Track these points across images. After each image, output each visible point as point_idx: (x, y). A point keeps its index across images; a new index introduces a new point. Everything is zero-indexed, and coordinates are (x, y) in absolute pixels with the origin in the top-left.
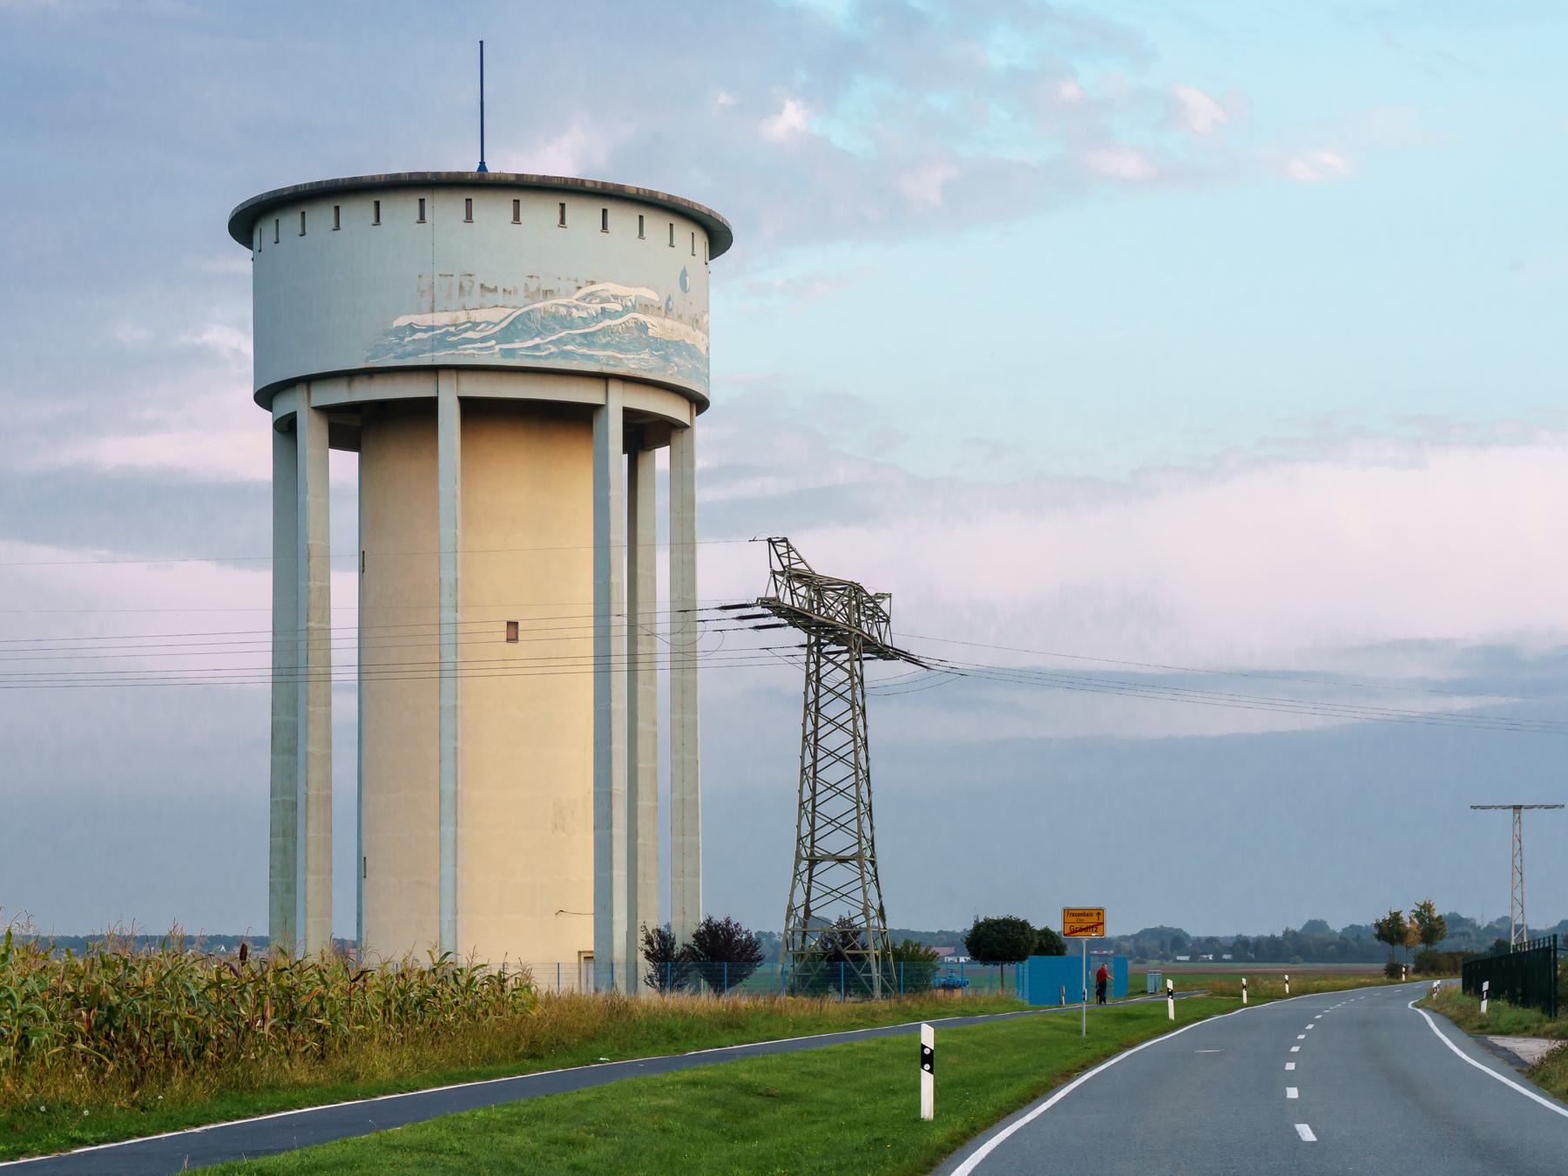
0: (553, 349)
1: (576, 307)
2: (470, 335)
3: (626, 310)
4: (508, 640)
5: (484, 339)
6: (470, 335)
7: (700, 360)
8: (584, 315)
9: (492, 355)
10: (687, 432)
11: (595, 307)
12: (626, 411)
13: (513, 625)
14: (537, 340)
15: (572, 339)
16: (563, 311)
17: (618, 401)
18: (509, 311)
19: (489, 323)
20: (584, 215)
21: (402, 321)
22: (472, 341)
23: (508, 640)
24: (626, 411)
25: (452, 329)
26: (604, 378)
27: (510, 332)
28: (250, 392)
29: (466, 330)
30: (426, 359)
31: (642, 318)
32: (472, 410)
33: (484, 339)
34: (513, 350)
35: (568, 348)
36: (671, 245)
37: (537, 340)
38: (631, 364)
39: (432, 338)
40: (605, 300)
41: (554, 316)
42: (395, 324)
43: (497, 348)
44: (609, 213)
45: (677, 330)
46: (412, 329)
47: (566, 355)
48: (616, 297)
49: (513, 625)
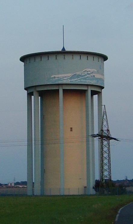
0: (79, 80)
1: (83, 73)
2: (65, 78)
3: (91, 73)
4: (71, 131)
5: (67, 79)
6: (65, 78)
7: (102, 80)
8: (84, 74)
9: (69, 82)
10: (101, 93)
11: (86, 73)
12: (91, 90)
13: (71, 128)
14: (76, 79)
15: (82, 79)
16: (81, 74)
17: (90, 89)
18: (71, 74)
19: (68, 76)
20: (84, 58)
21: (53, 76)
22: (65, 79)
23: (71, 131)
24: (91, 90)
25: (62, 78)
26: (88, 85)
27: (71, 78)
28: (24, 88)
29: (64, 78)
30: (57, 83)
31: (94, 74)
32: (64, 91)
33: (67, 79)
34: (72, 81)
35: (82, 80)
36: (98, 61)
37: (76, 79)
38: (93, 82)
39: (58, 79)
40: (88, 72)
41: (79, 75)
42: (52, 77)
43: (70, 80)
44: (94, 58)
45: (98, 76)
46: (55, 77)
47: (81, 81)
48: (89, 71)
49: (71, 128)
